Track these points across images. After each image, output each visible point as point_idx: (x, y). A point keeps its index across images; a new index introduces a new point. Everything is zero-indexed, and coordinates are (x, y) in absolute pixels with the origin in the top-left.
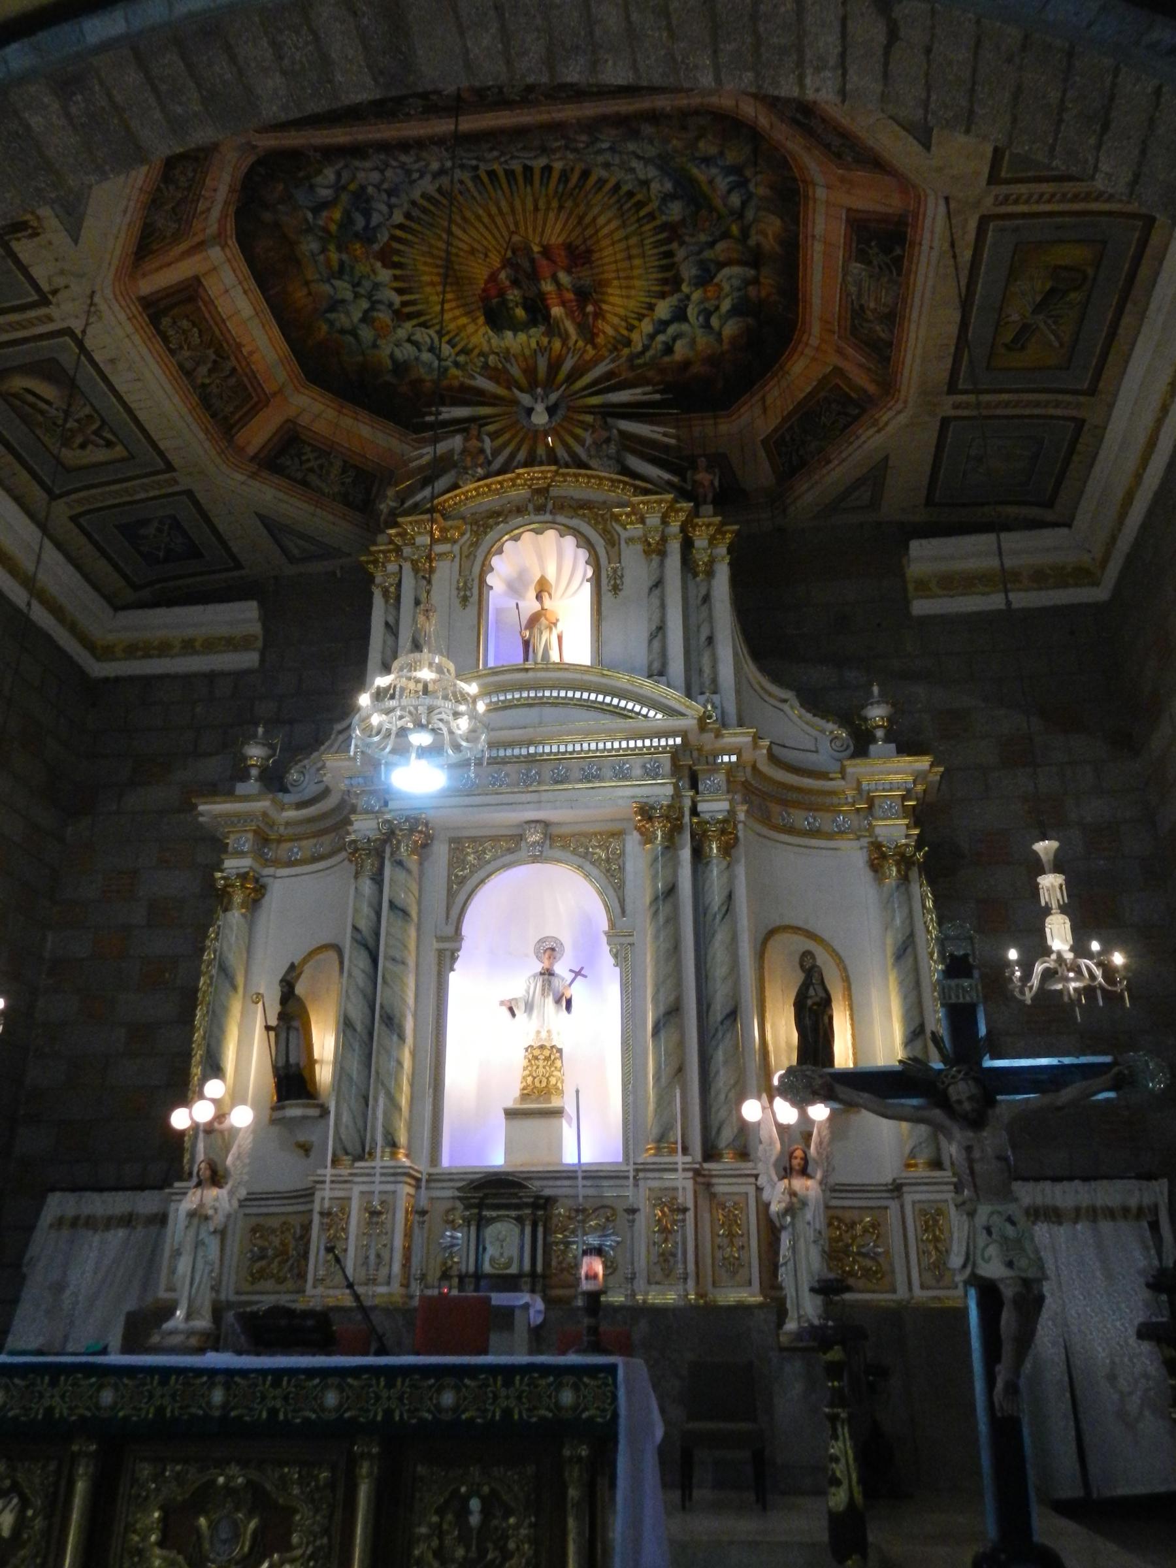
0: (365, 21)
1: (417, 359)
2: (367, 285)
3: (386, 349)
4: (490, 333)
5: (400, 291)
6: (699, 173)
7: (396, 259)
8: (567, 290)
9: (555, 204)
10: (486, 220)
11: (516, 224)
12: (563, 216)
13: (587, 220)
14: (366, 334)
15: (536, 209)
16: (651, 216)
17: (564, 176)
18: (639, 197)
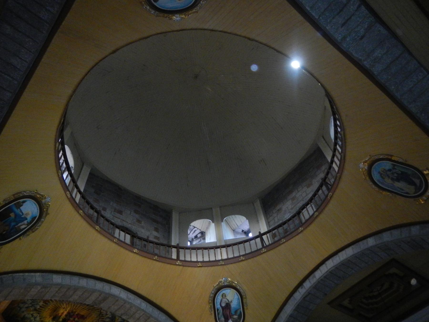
0: (100, 297)
1: (30, 318)
2: (35, 303)
3: (25, 313)
4: (51, 320)
5: (41, 307)
6: (117, 318)
7: (47, 302)
8: (75, 321)
9: (88, 309)
10: (72, 305)
11: (77, 309)
12: (87, 311)
13: (91, 314)
14: (23, 309)
15: (84, 309)
16: (103, 319)
17: (94, 308)
18: (104, 315)
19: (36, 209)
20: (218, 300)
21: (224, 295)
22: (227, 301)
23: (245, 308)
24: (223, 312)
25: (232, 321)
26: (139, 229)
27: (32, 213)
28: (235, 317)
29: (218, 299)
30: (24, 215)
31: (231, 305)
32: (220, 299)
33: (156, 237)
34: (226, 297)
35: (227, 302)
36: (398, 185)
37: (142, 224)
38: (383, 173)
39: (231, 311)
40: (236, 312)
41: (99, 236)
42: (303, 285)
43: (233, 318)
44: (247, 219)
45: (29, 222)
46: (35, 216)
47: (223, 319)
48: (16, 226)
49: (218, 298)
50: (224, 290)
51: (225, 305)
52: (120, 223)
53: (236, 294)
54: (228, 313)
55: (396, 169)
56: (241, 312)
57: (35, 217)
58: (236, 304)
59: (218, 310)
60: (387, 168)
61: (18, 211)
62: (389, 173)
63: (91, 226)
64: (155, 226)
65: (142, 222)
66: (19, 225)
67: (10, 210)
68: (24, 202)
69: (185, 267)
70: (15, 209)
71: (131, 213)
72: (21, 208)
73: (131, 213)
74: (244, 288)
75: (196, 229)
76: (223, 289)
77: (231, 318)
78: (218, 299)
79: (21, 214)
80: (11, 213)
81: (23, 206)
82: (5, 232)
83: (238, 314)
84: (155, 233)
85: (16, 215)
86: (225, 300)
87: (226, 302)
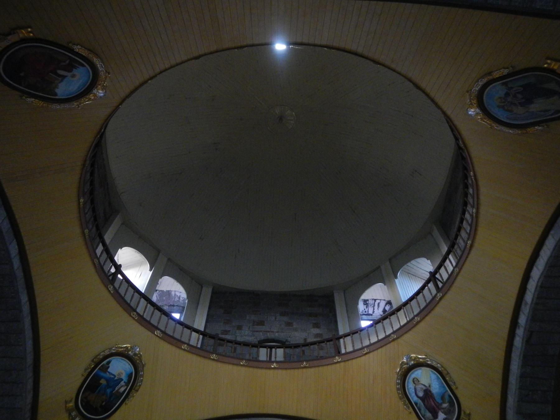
19: (127, 365)
20: (411, 389)
21: (415, 380)
22: (423, 387)
23: (453, 387)
24: (424, 405)
25: (442, 413)
26: (290, 333)
27: (125, 371)
28: (445, 405)
29: (410, 388)
30: (117, 376)
31: (432, 390)
32: (413, 388)
33: (317, 335)
34: (419, 381)
35: (424, 388)
36: (537, 106)
37: (294, 326)
38: (503, 104)
39: (435, 400)
40: (443, 398)
41: (220, 365)
42: (519, 323)
43: (443, 409)
44: (428, 259)
45: (126, 381)
46: (130, 372)
47: (429, 415)
48: (114, 392)
49: (409, 387)
50: (413, 373)
51: (423, 394)
52: (262, 336)
53: (431, 373)
54: (433, 404)
55: (512, 88)
56: (450, 396)
57: (131, 374)
58: (437, 386)
59: (416, 404)
60: (502, 93)
61: (107, 375)
62: (509, 99)
63: (205, 357)
64: (314, 322)
65: (294, 323)
66: (116, 389)
67: (97, 378)
68: (109, 363)
69: (347, 363)
70: (102, 374)
71: (276, 318)
72: (109, 370)
73: (276, 318)
74: (438, 360)
75: (377, 301)
76: (411, 373)
77: (439, 409)
78: (410, 388)
79: (113, 377)
80: (100, 380)
81: (110, 367)
82: (104, 403)
83: (447, 401)
84: (316, 331)
85: (108, 380)
86: (420, 386)
87: (422, 388)
